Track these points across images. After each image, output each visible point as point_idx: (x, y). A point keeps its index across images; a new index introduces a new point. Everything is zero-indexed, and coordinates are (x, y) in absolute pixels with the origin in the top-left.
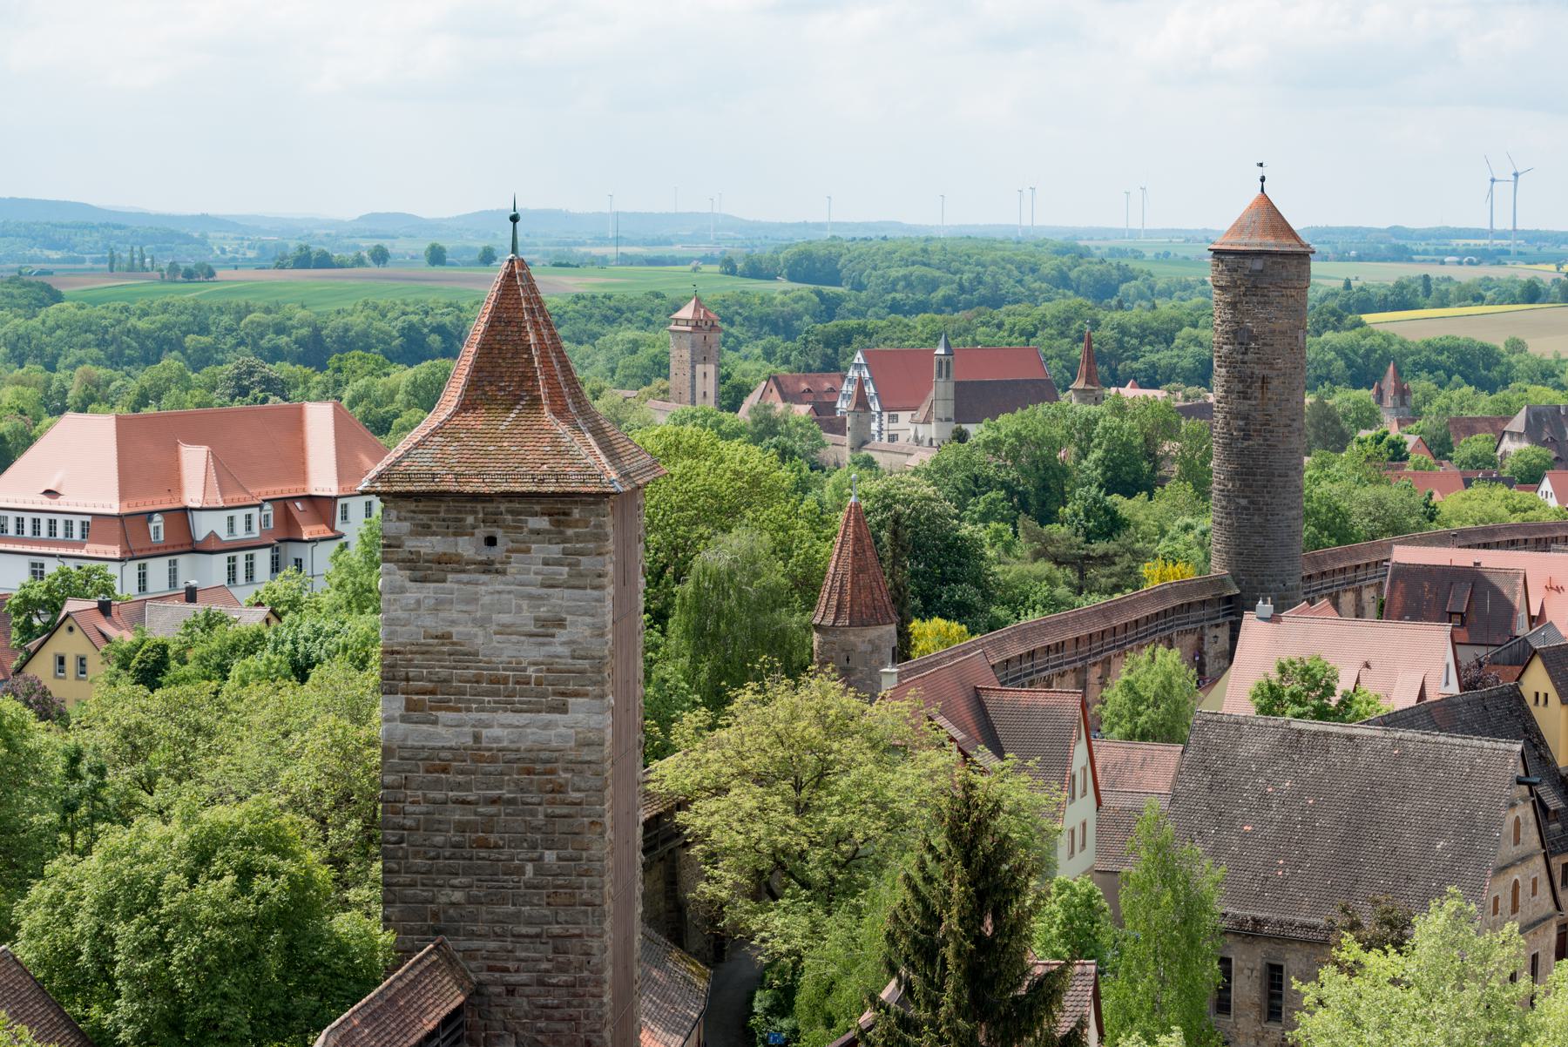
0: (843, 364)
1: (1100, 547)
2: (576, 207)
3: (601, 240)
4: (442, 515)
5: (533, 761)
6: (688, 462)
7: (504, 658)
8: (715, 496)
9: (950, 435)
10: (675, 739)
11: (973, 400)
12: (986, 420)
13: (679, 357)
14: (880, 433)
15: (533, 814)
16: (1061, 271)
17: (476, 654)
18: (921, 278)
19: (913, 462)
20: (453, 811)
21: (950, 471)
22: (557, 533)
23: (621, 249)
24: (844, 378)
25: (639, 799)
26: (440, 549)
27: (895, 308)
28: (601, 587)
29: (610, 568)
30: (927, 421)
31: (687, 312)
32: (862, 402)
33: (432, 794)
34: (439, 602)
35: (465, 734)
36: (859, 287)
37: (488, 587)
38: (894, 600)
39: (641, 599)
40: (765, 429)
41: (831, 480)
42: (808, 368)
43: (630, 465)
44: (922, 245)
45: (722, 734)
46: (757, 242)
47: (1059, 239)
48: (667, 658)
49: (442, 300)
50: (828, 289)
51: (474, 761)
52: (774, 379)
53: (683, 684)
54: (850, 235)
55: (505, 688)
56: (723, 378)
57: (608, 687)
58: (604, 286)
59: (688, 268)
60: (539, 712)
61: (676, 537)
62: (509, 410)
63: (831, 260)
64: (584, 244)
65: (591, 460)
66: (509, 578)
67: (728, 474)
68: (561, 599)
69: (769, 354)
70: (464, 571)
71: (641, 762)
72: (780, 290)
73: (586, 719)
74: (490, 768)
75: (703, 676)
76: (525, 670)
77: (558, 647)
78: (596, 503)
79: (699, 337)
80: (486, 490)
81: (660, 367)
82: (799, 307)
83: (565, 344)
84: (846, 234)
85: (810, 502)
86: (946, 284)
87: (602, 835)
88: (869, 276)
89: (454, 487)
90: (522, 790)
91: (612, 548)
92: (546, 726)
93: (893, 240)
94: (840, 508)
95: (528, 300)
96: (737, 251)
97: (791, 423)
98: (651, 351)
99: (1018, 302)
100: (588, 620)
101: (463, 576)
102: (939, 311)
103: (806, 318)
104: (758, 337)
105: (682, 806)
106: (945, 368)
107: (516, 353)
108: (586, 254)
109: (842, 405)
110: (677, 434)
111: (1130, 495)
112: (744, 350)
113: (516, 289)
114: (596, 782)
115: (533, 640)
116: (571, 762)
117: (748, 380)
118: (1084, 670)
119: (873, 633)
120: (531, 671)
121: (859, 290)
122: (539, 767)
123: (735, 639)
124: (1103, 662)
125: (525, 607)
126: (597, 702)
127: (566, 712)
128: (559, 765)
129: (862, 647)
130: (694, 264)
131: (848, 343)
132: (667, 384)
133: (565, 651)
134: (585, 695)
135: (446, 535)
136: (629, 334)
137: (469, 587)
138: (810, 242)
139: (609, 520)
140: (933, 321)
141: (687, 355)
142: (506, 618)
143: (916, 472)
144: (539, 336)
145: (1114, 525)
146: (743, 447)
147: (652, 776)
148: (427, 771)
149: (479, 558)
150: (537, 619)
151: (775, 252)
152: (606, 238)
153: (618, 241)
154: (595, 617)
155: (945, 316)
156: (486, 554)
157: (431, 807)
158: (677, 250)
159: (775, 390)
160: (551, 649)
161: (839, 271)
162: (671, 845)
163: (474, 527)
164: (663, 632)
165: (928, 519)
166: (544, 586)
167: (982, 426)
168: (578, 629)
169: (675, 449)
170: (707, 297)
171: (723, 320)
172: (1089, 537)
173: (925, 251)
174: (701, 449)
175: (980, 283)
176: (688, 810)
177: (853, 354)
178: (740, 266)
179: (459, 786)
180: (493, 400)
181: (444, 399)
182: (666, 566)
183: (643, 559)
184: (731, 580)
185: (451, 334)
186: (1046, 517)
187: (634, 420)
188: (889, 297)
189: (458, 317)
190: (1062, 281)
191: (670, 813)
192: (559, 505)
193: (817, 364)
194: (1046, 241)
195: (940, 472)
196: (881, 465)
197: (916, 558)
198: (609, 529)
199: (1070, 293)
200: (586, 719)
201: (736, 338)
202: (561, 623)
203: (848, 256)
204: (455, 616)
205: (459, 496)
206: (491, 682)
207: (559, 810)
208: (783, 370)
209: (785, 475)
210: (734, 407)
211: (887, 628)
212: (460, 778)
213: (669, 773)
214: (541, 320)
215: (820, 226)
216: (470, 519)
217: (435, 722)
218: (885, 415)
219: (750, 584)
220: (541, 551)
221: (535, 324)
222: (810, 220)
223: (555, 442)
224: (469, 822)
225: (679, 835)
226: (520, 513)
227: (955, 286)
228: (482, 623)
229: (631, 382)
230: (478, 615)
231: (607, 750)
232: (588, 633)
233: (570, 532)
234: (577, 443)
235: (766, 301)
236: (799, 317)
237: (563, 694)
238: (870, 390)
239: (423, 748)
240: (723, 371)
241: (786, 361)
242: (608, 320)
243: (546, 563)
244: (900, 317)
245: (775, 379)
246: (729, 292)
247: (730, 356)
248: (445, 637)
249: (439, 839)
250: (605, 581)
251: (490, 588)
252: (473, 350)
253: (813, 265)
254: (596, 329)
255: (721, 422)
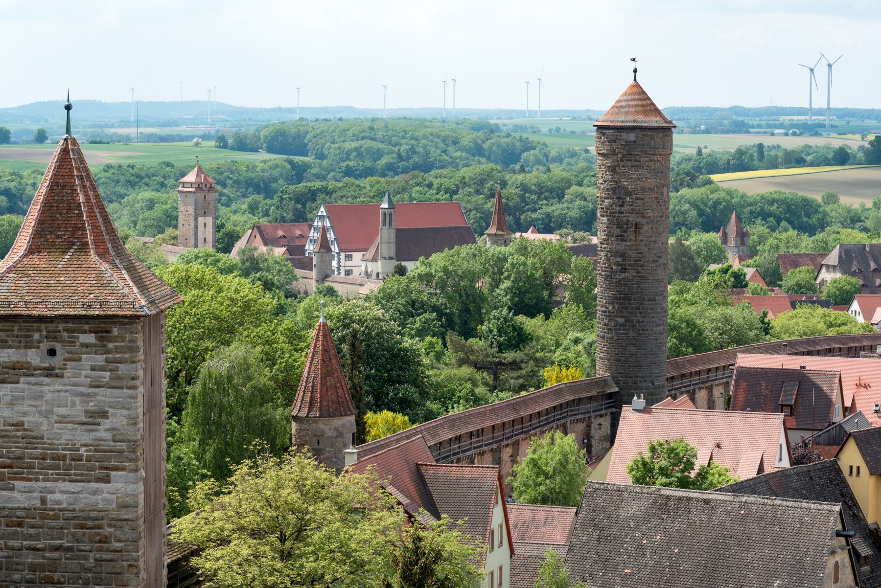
0: (309, 216)
1: (510, 356)
2: (107, 99)
3: (125, 123)
4: (16, 332)
5: (85, 519)
6: (195, 292)
7: (63, 441)
8: (216, 318)
9: (392, 270)
10: (191, 502)
11: (411, 243)
12: (421, 258)
13: (186, 211)
14: (339, 268)
15: (86, 558)
16: (476, 144)
17: (42, 438)
18: (369, 150)
19: (364, 291)
20: (27, 556)
21: (393, 298)
22: (101, 347)
23: (141, 130)
24: (310, 226)
25: (164, 548)
26: (15, 358)
27: (349, 172)
28: (134, 388)
29: (141, 373)
30: (374, 260)
31: (191, 177)
32: (325, 245)
33: (12, 543)
34: (14, 398)
35: (34, 498)
36: (321, 156)
37: (50, 387)
38: (353, 397)
39: (164, 395)
40: (251, 266)
41: (302, 305)
42: (283, 220)
43: (155, 294)
44: (369, 124)
45: (225, 499)
46: (243, 123)
47: (475, 118)
48: (180, 441)
49: (7, 170)
50: (297, 159)
51: (42, 518)
52: (258, 228)
53: (194, 462)
54: (314, 117)
55: (63, 464)
56: (219, 228)
57: (140, 463)
58: (128, 158)
59: (191, 143)
60: (90, 482)
61: (188, 349)
62: (65, 252)
63: (299, 136)
64: (112, 126)
65: (126, 291)
66: (66, 380)
67: (228, 302)
68: (104, 396)
69: (253, 209)
70: (32, 375)
71: (165, 521)
72: (262, 159)
73: (124, 487)
74: (54, 523)
75: (208, 456)
76: (78, 450)
77: (103, 433)
78: (130, 324)
79: (201, 196)
80: (48, 313)
81: (171, 219)
82: (276, 173)
83: (105, 203)
84: (312, 117)
85: (287, 322)
86: (388, 153)
87: (137, 574)
88: (329, 149)
89: (24, 312)
90: (78, 541)
91: (142, 357)
92: (95, 492)
93: (347, 120)
94: (310, 326)
95: (78, 169)
96: (228, 130)
97: (271, 261)
98: (164, 207)
99: (442, 167)
100: (125, 412)
101: (32, 379)
102: (383, 175)
103: (281, 181)
104: (244, 196)
105: (196, 553)
106: (388, 219)
107: (70, 209)
108: (114, 134)
109: (310, 248)
110: (187, 271)
111: (531, 313)
112: (234, 206)
113: (69, 159)
114: (132, 535)
115: (84, 427)
116: (113, 519)
117: (238, 228)
118: (499, 450)
119: (338, 422)
120: (82, 451)
121: (323, 160)
122: (89, 523)
123: (233, 427)
124: (513, 444)
125: (78, 402)
126: (132, 475)
127: (109, 482)
128: (105, 522)
129: (330, 433)
130: (195, 140)
131: (314, 200)
132: (177, 232)
133: (108, 435)
134: (123, 469)
135: (18, 348)
136: (147, 194)
137: (37, 388)
138: (283, 123)
139: (139, 336)
140: (378, 182)
141: (191, 210)
142: (63, 411)
143: (367, 298)
144: (87, 196)
145: (520, 339)
146: (237, 280)
147: (173, 530)
148: (7, 526)
149: (43, 365)
150: (86, 412)
151: (257, 130)
152: (129, 122)
153: (138, 123)
154: (129, 411)
155: (388, 179)
156: (49, 362)
157: (11, 553)
158: (183, 130)
159: (258, 236)
160: (98, 435)
161: (306, 145)
162: (187, 583)
163: (40, 342)
164: (178, 422)
165: (377, 334)
166: (92, 386)
167: (418, 263)
168: (118, 419)
169: (185, 282)
170: (206, 166)
171: (219, 183)
172: (501, 348)
173: (371, 128)
174: (205, 282)
175: (414, 152)
176: (200, 556)
177: (317, 208)
178: (230, 141)
179: (31, 537)
180: (53, 245)
181: (16, 245)
182: (180, 371)
183: (164, 366)
184: (229, 382)
185: (14, 195)
186: (468, 333)
187: (151, 260)
188: (344, 164)
189: (20, 183)
190: (478, 151)
191: (186, 558)
192: (103, 326)
193: (290, 216)
194: (464, 121)
195: (385, 298)
196: (340, 293)
197: (369, 365)
198: (140, 343)
199: (484, 160)
200: (124, 487)
201: (228, 196)
202: (104, 415)
203: (312, 134)
204: (26, 409)
205: (29, 318)
206: (53, 459)
207: (105, 556)
208: (264, 221)
209: (269, 301)
210: (227, 249)
211: (348, 418)
212: (32, 531)
213: (185, 528)
214: (88, 184)
215: (291, 110)
216: (36, 336)
217: (12, 489)
218: (343, 255)
219: (244, 385)
220: (89, 360)
221: (84, 187)
222: (283, 106)
223: (99, 276)
224: (38, 564)
225: (193, 575)
226: (73, 331)
227: (394, 155)
228: (46, 414)
229: (149, 231)
230: (43, 408)
231: (140, 511)
232: (125, 422)
233: (111, 345)
234: (116, 278)
235: (250, 168)
236: (275, 180)
237: (107, 468)
238: (331, 236)
239: (4, 508)
240: (218, 222)
241: (266, 214)
242: (132, 184)
243: (93, 369)
244: (352, 180)
245: (259, 228)
246: (222, 162)
247: (223, 210)
248: (19, 425)
249: (17, 576)
250: (138, 382)
251: (52, 388)
252: (38, 207)
253: (286, 140)
254: (123, 191)
255: (218, 261)
